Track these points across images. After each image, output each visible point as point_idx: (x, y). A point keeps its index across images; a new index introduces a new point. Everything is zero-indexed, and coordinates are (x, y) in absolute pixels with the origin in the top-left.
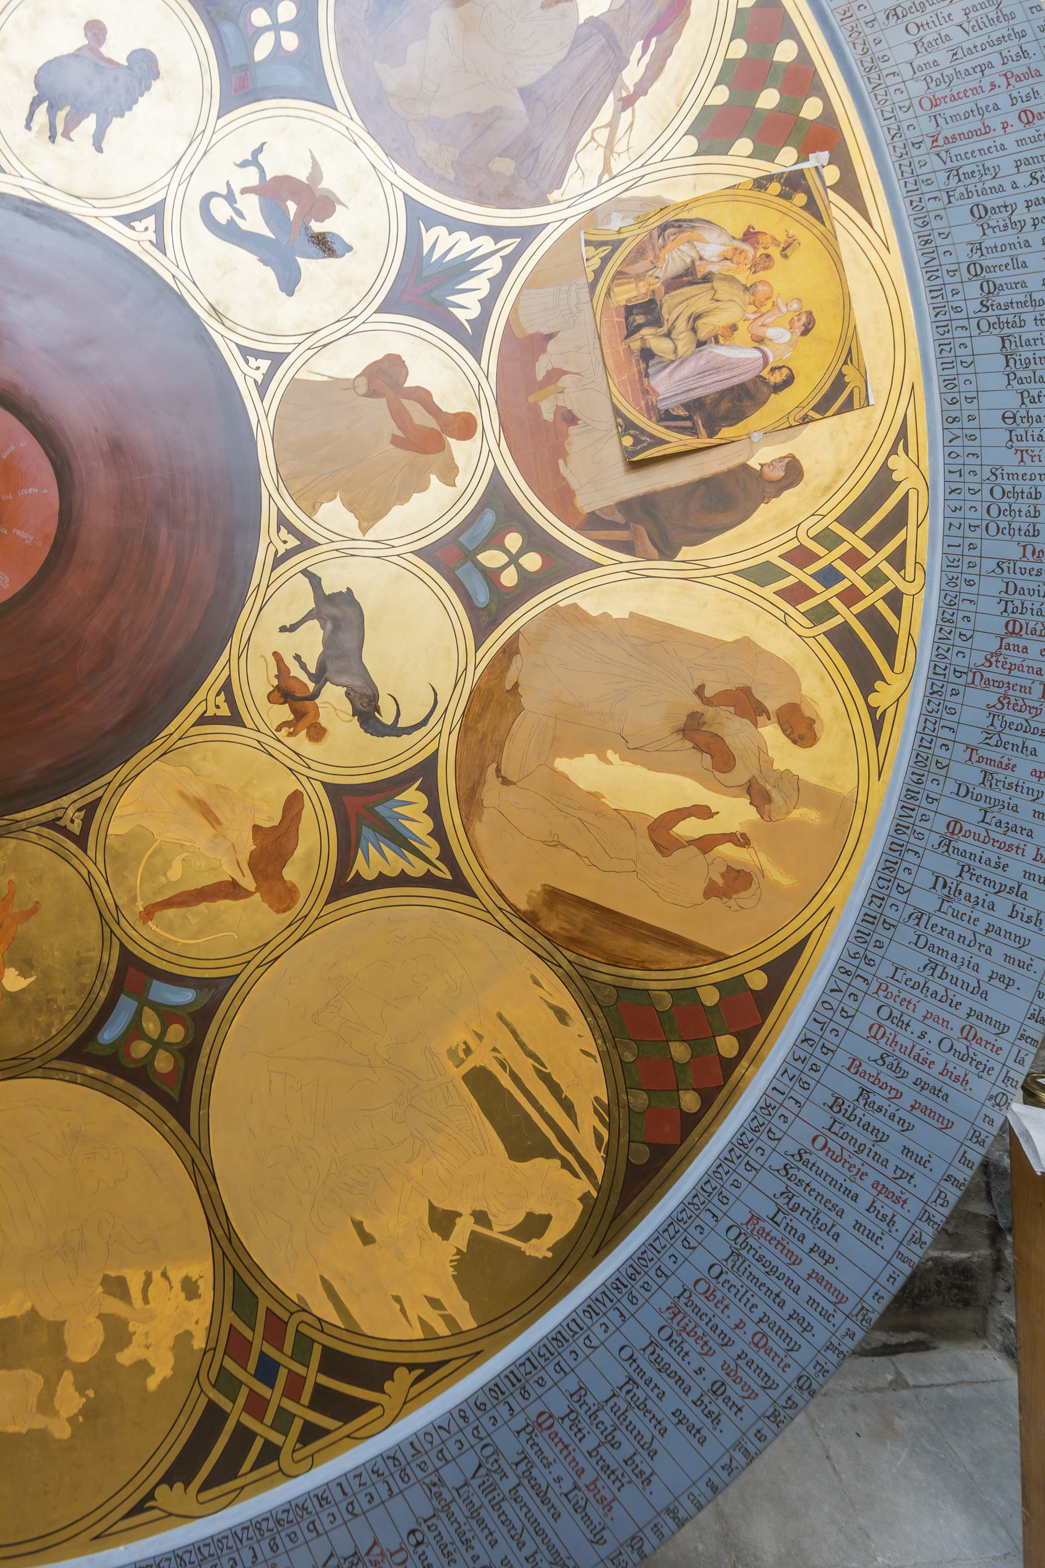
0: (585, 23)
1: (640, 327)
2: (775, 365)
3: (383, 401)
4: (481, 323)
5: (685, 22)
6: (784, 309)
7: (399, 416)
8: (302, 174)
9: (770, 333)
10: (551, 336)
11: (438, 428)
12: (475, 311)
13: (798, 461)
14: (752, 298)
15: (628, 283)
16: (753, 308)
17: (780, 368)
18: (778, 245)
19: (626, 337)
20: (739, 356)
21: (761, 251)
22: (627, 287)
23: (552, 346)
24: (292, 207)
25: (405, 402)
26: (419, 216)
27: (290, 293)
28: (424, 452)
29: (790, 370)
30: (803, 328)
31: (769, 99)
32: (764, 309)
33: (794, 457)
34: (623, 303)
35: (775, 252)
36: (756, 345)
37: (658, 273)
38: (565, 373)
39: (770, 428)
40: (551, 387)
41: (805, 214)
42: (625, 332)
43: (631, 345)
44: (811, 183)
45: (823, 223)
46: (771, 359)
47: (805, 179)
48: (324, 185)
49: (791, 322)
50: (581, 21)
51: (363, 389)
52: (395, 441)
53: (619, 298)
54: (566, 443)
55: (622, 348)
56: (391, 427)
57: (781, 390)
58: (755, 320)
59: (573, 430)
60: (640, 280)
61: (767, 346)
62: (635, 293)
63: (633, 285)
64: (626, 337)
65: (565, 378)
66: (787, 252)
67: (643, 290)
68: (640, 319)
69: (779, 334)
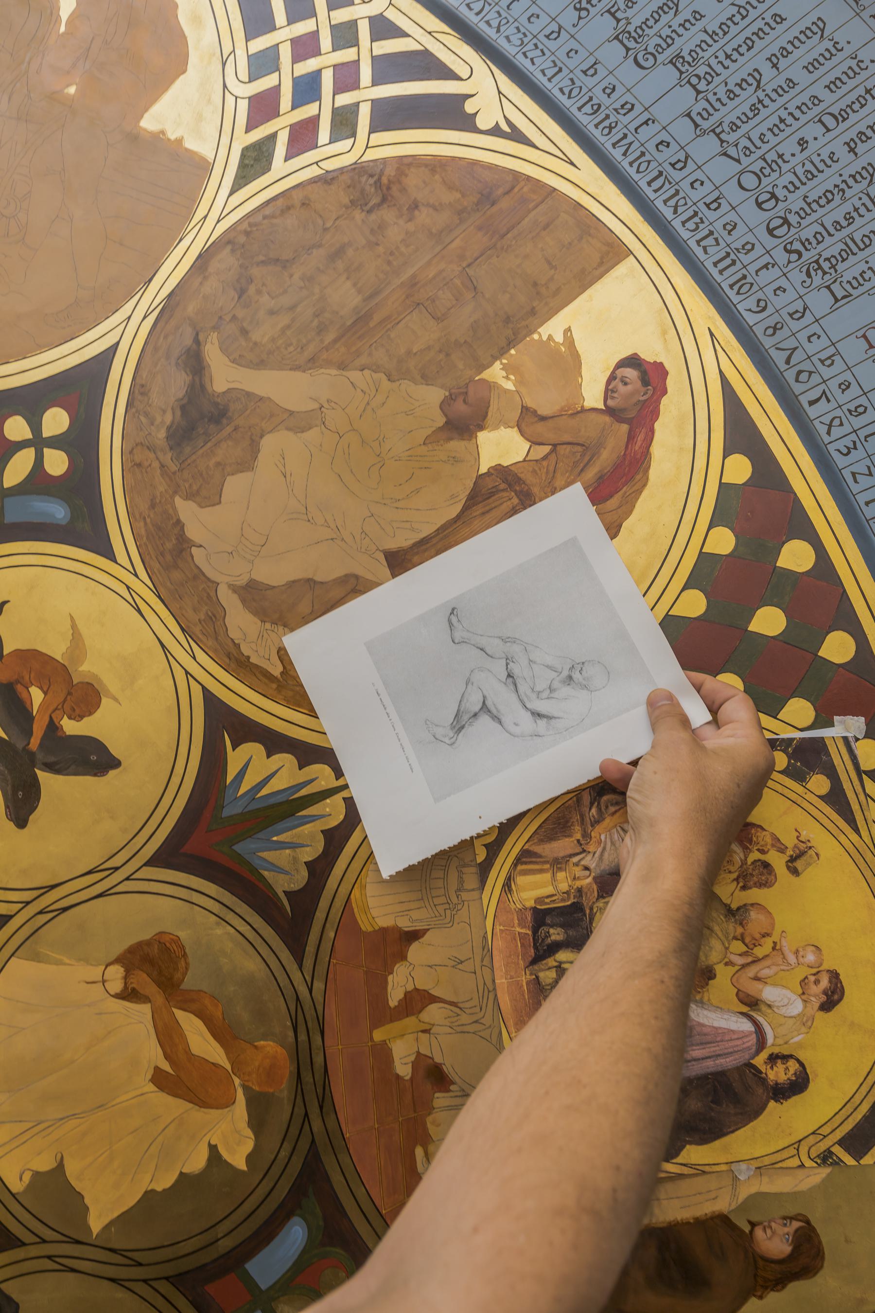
0: (488, 474)
1: (555, 948)
2: (776, 1050)
3: (146, 1008)
4: (307, 898)
5: (639, 492)
6: (792, 959)
7: (169, 1037)
8: (57, 649)
9: (769, 993)
10: (414, 936)
11: (228, 1067)
12: (301, 878)
13: (814, 1230)
14: (740, 930)
15: (541, 871)
16: (738, 946)
17: (785, 1058)
18: (782, 850)
19: (535, 961)
20: (716, 1024)
21: (755, 856)
22: (538, 877)
23: (415, 951)
24: (37, 696)
25: (179, 1014)
26: (225, 725)
27: (21, 822)
28: (202, 1103)
29: (802, 1064)
30: (824, 998)
31: (769, 621)
32: (759, 952)
33: (808, 1222)
34: (531, 904)
35: (777, 860)
36: (745, 1009)
37: (588, 861)
38: (434, 999)
39: (767, 1161)
40: (410, 1022)
41: (827, 810)
42: (532, 952)
43: (541, 975)
44: (837, 761)
45: (857, 831)
46: (770, 1040)
47: (828, 754)
48: (84, 668)
49: (804, 982)
50: (483, 469)
51: (116, 986)
52: (159, 1079)
53: (525, 895)
54: (429, 1120)
55: (525, 978)
56: (153, 1054)
57: (786, 1097)
58: (743, 966)
59: (440, 1100)
60: (560, 869)
61: (764, 1015)
62: (550, 890)
63: (548, 876)
64: (535, 961)
65: (433, 1008)
66: (799, 864)
67: (564, 887)
68: (556, 934)
69: (784, 999)
